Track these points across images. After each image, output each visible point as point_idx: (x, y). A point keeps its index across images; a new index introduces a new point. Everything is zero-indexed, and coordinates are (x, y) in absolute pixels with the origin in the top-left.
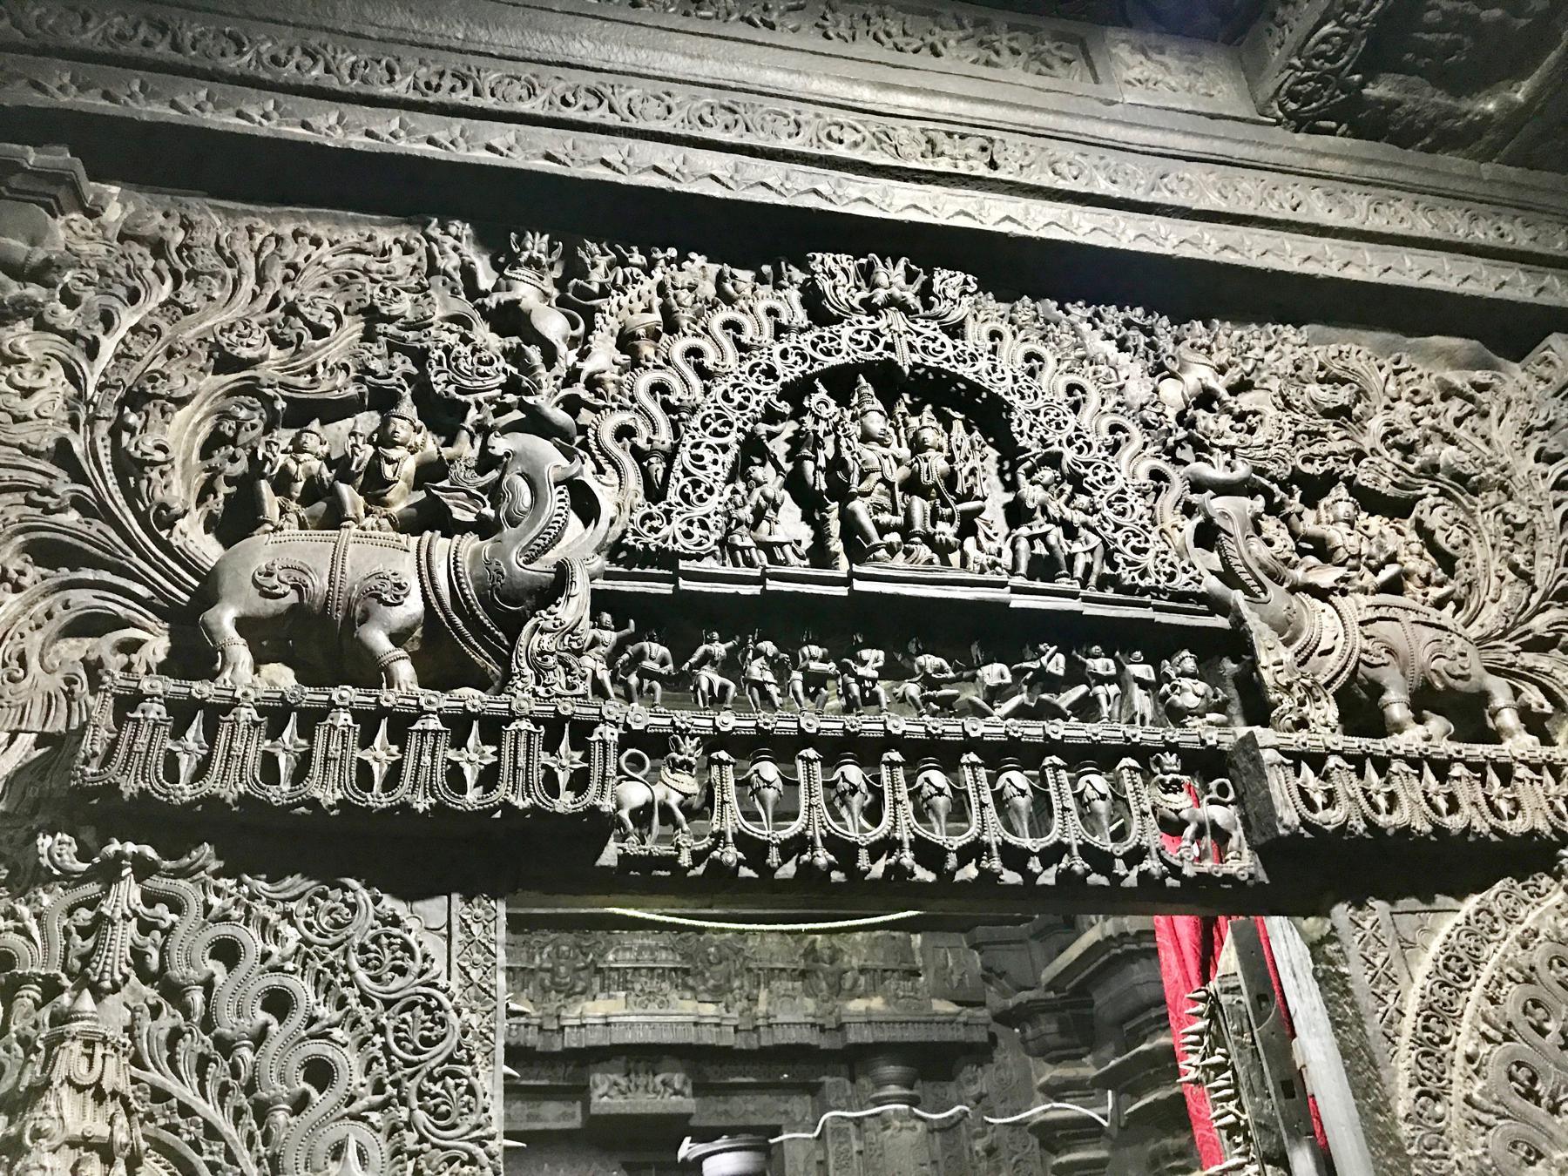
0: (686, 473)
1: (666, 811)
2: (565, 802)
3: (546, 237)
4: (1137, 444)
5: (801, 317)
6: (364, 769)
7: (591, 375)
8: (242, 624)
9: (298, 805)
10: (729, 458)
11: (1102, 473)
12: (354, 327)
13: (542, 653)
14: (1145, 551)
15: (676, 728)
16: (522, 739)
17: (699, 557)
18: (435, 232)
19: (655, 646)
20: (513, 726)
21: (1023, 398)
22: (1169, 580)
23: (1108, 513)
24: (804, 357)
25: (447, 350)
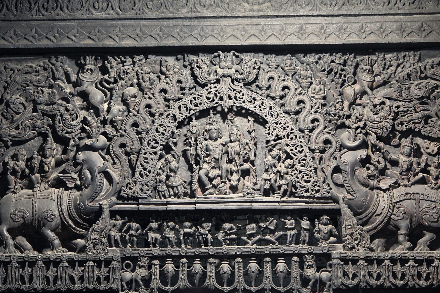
0: (142, 166)
1: (137, 281)
2: (103, 287)
3: (94, 57)
4: (321, 128)
5: (190, 82)
6: (47, 278)
7: (112, 120)
8: (9, 231)
9: (31, 290)
10: (157, 157)
11: (298, 149)
12: (30, 108)
13: (95, 239)
14: (309, 181)
15: (140, 255)
16: (90, 268)
17: (146, 198)
18: (54, 61)
19: (134, 224)
20: (87, 264)
21: (272, 116)
22: (316, 193)
23: (298, 166)
24: (187, 108)
25: (62, 116)
